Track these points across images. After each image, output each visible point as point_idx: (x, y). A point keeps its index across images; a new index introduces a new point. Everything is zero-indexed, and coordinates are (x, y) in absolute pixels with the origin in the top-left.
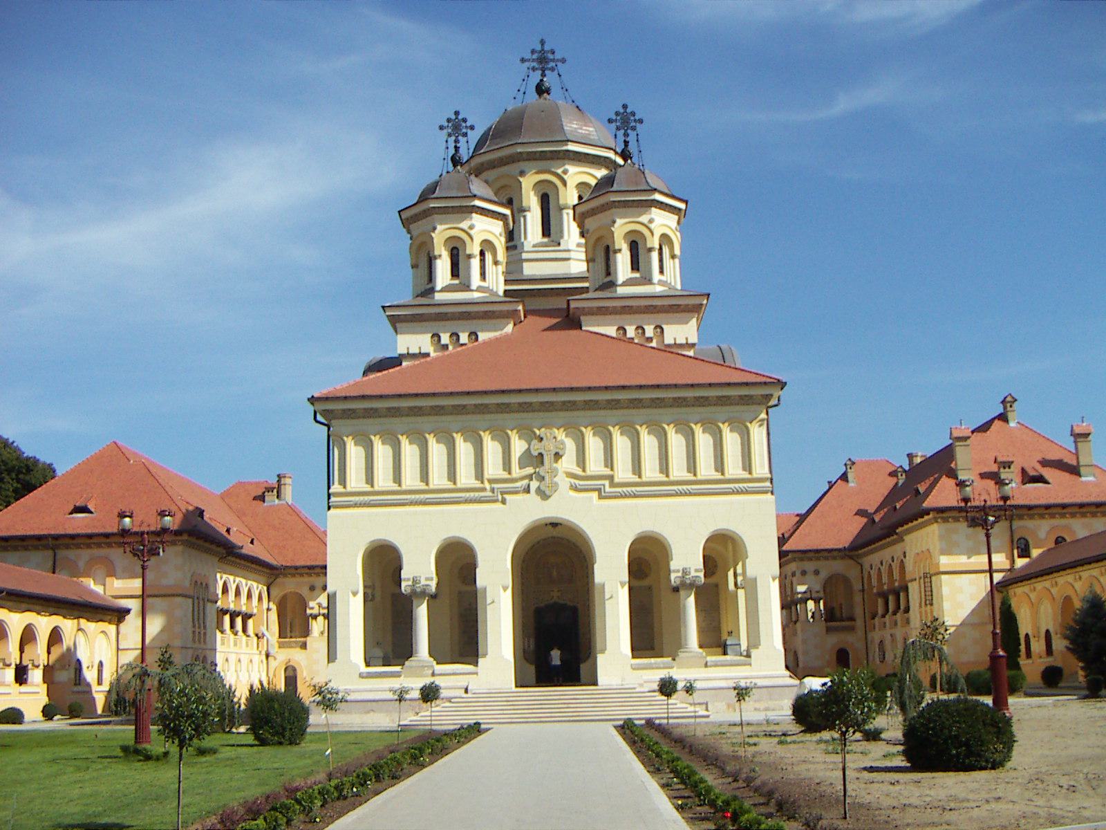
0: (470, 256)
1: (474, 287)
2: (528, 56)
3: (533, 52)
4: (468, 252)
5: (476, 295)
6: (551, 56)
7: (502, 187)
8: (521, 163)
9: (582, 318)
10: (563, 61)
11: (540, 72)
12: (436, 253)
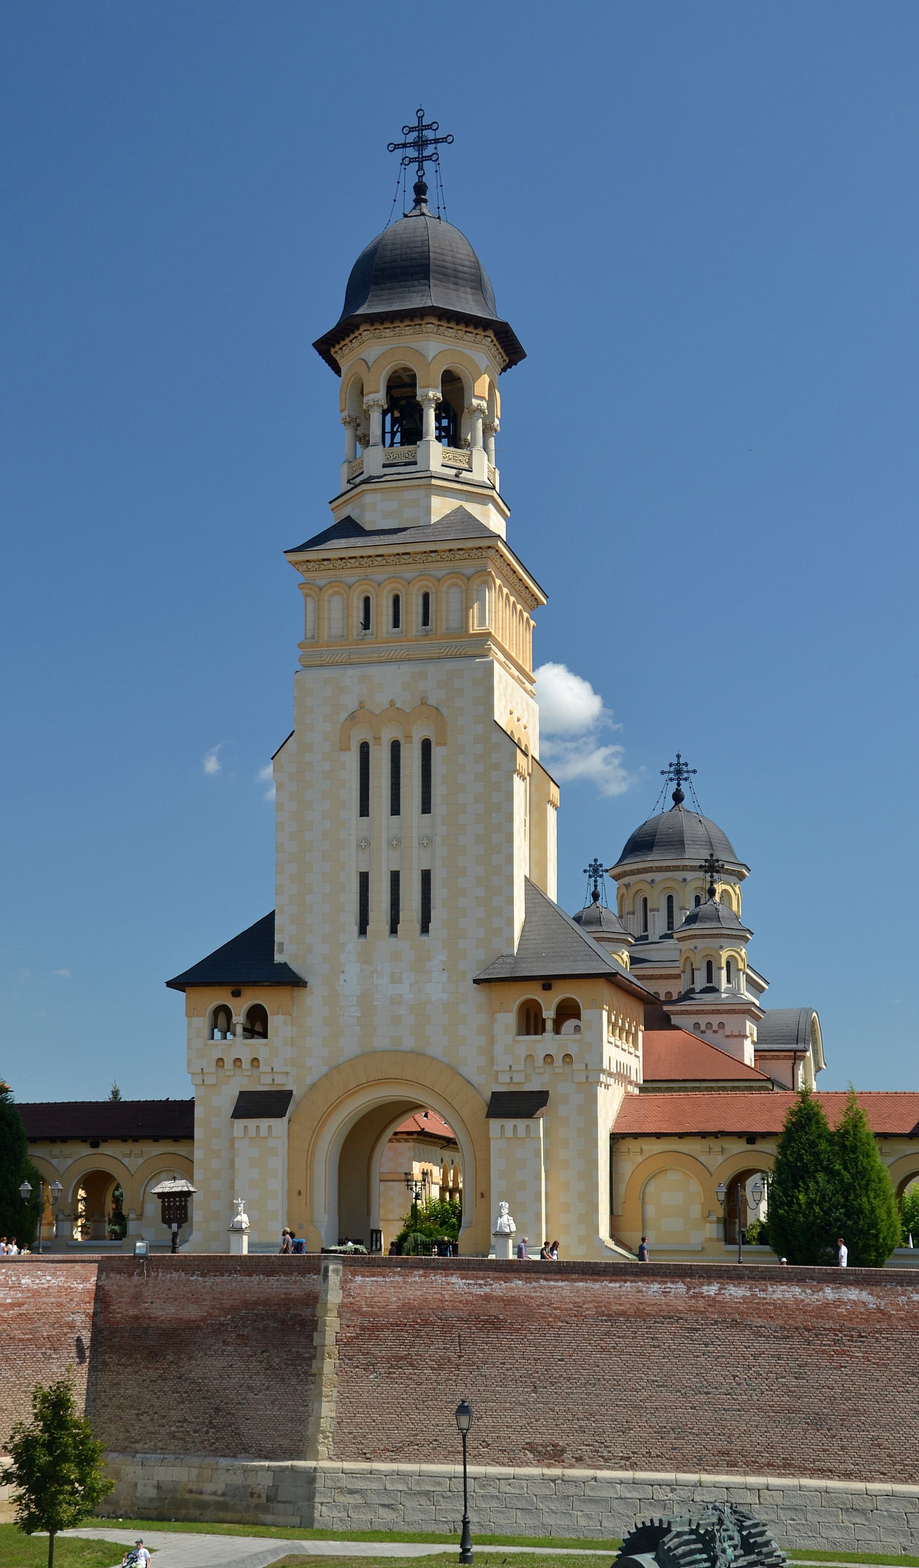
2: (667, 769)
3: (671, 765)
6: (685, 768)
8: (652, 874)
9: (671, 1016)
10: (695, 772)
11: (677, 782)
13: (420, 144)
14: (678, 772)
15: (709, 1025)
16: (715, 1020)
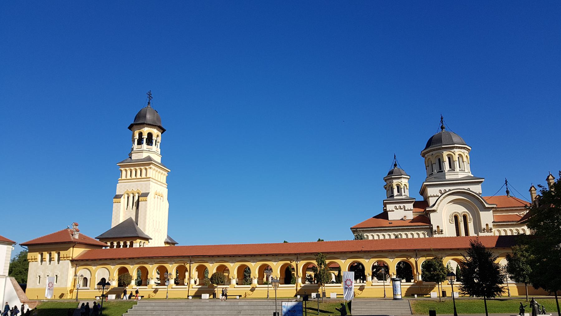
0: (401, 188)
1: (403, 195)
4: (401, 187)
5: (404, 197)
7: (436, 156)
12: (394, 188)
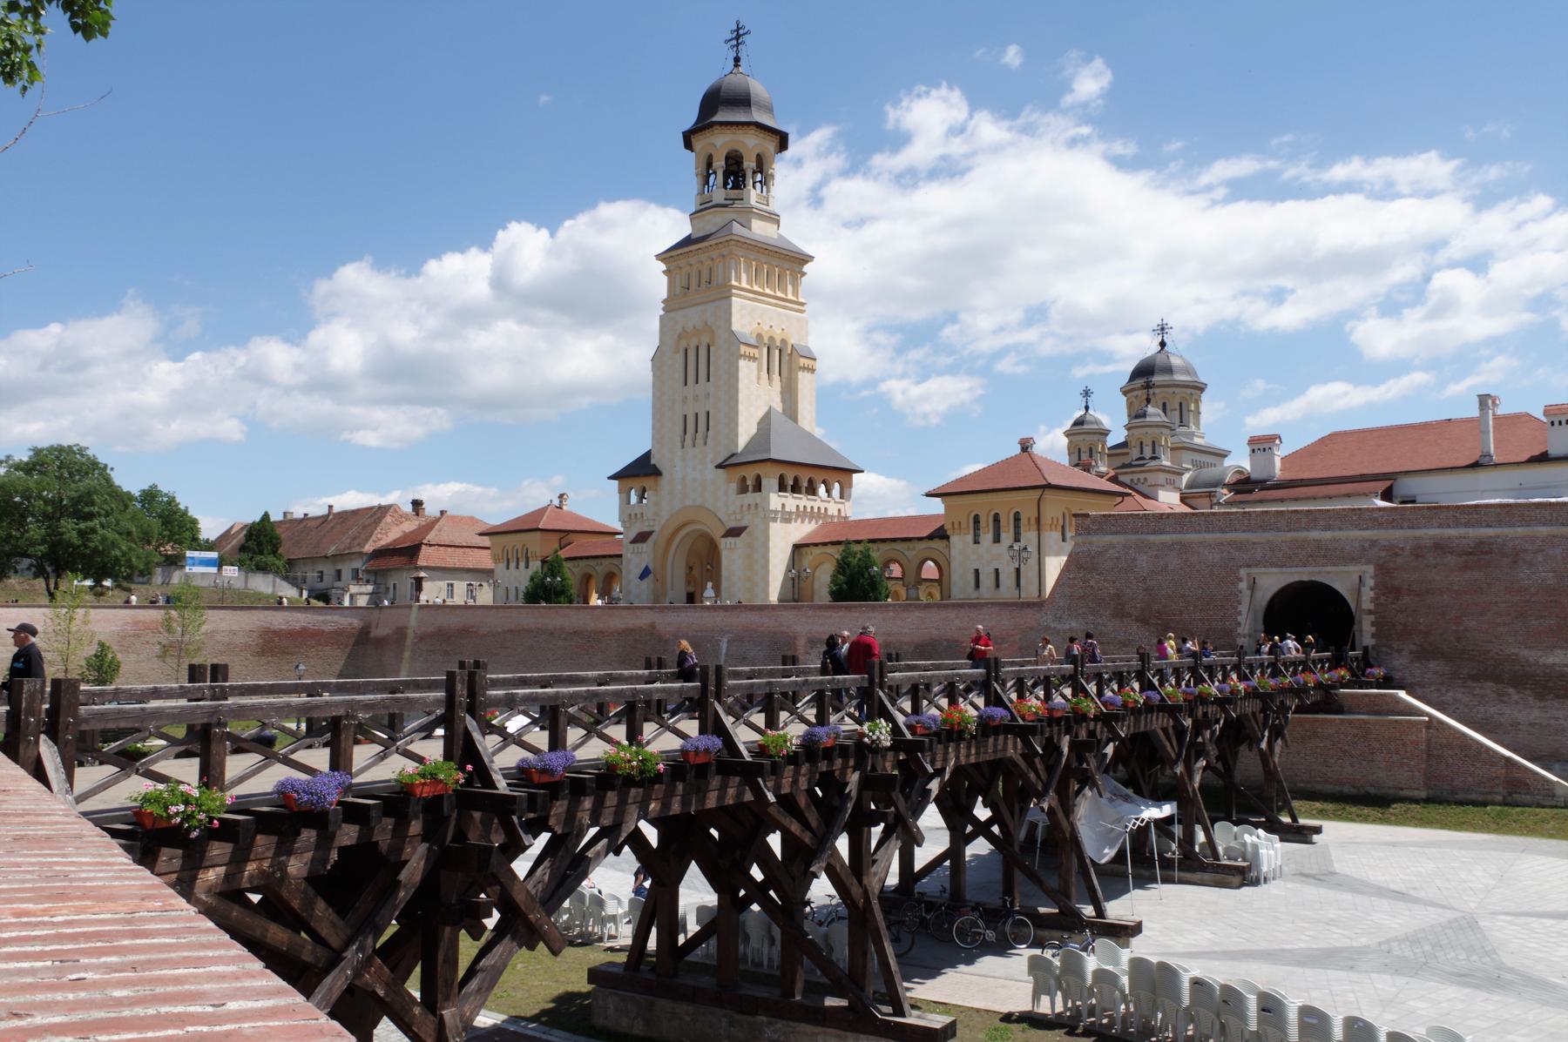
13: (737, 38)
14: (1163, 329)
15: (1139, 480)
16: (1142, 476)
